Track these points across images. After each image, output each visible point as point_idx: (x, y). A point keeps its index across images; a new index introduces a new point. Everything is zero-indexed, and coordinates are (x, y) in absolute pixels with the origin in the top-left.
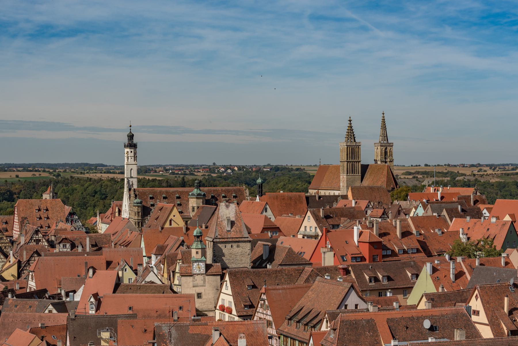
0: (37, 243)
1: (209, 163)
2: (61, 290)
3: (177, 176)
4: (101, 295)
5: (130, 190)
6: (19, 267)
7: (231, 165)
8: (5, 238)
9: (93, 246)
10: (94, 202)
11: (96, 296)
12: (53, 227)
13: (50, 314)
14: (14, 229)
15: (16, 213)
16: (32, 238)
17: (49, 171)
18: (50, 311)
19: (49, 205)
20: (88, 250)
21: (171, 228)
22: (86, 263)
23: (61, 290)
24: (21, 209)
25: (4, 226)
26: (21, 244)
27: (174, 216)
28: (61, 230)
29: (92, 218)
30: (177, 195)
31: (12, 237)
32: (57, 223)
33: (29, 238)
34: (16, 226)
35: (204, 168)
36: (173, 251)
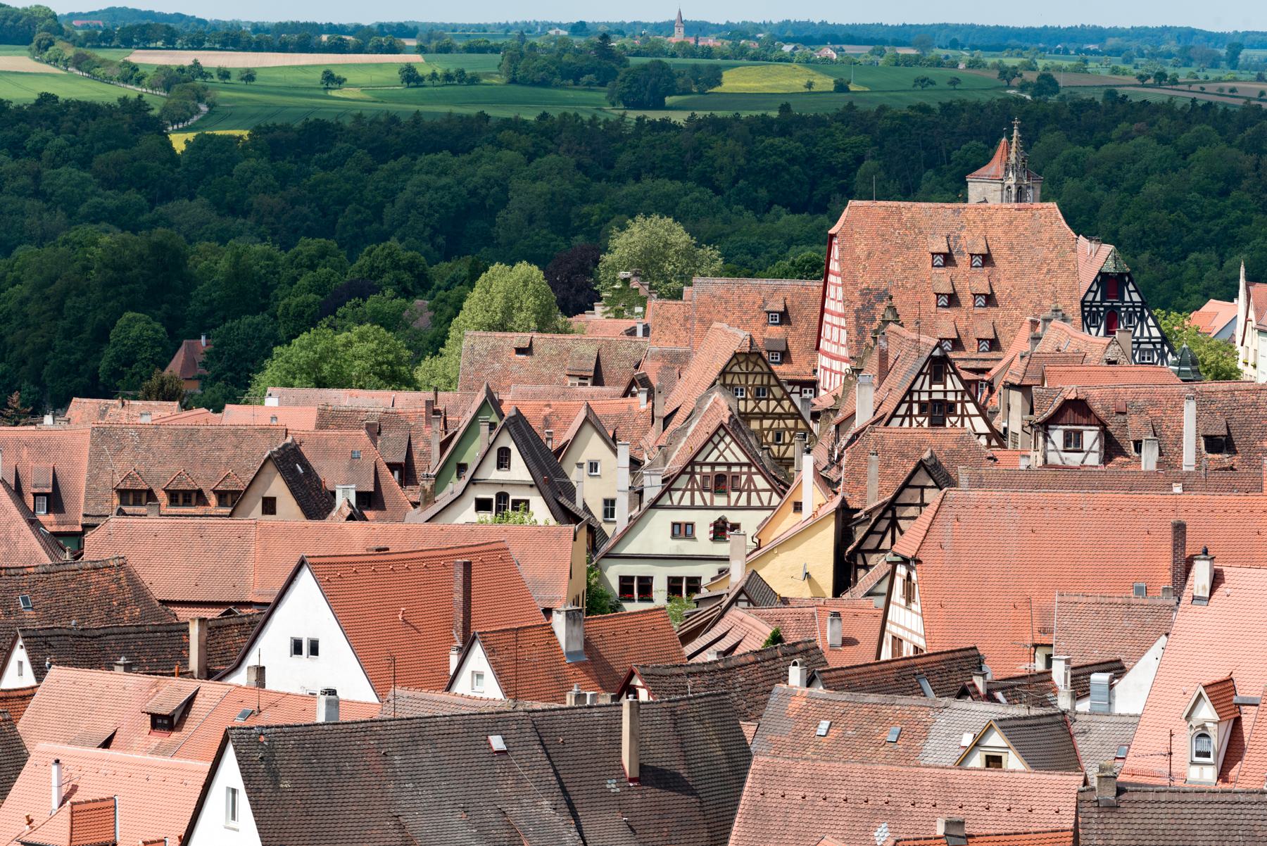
0: (937, 422)
2: (1049, 660)
4: (1245, 690)
6: (843, 537)
8: (777, 392)
9: (1214, 444)
10: (1224, 221)
11: (1222, 692)
12: (1017, 345)
13: (992, 774)
14: (824, 345)
15: (834, 266)
16: (910, 392)
18: (994, 761)
20: (1188, 459)
22: (1179, 529)
23: (1049, 660)
24: (861, 250)
25: (776, 332)
26: (858, 424)
28: (1059, 357)
29: (1213, 305)
31: (813, 385)
32: (1034, 324)
33: (899, 394)
34: (836, 336)
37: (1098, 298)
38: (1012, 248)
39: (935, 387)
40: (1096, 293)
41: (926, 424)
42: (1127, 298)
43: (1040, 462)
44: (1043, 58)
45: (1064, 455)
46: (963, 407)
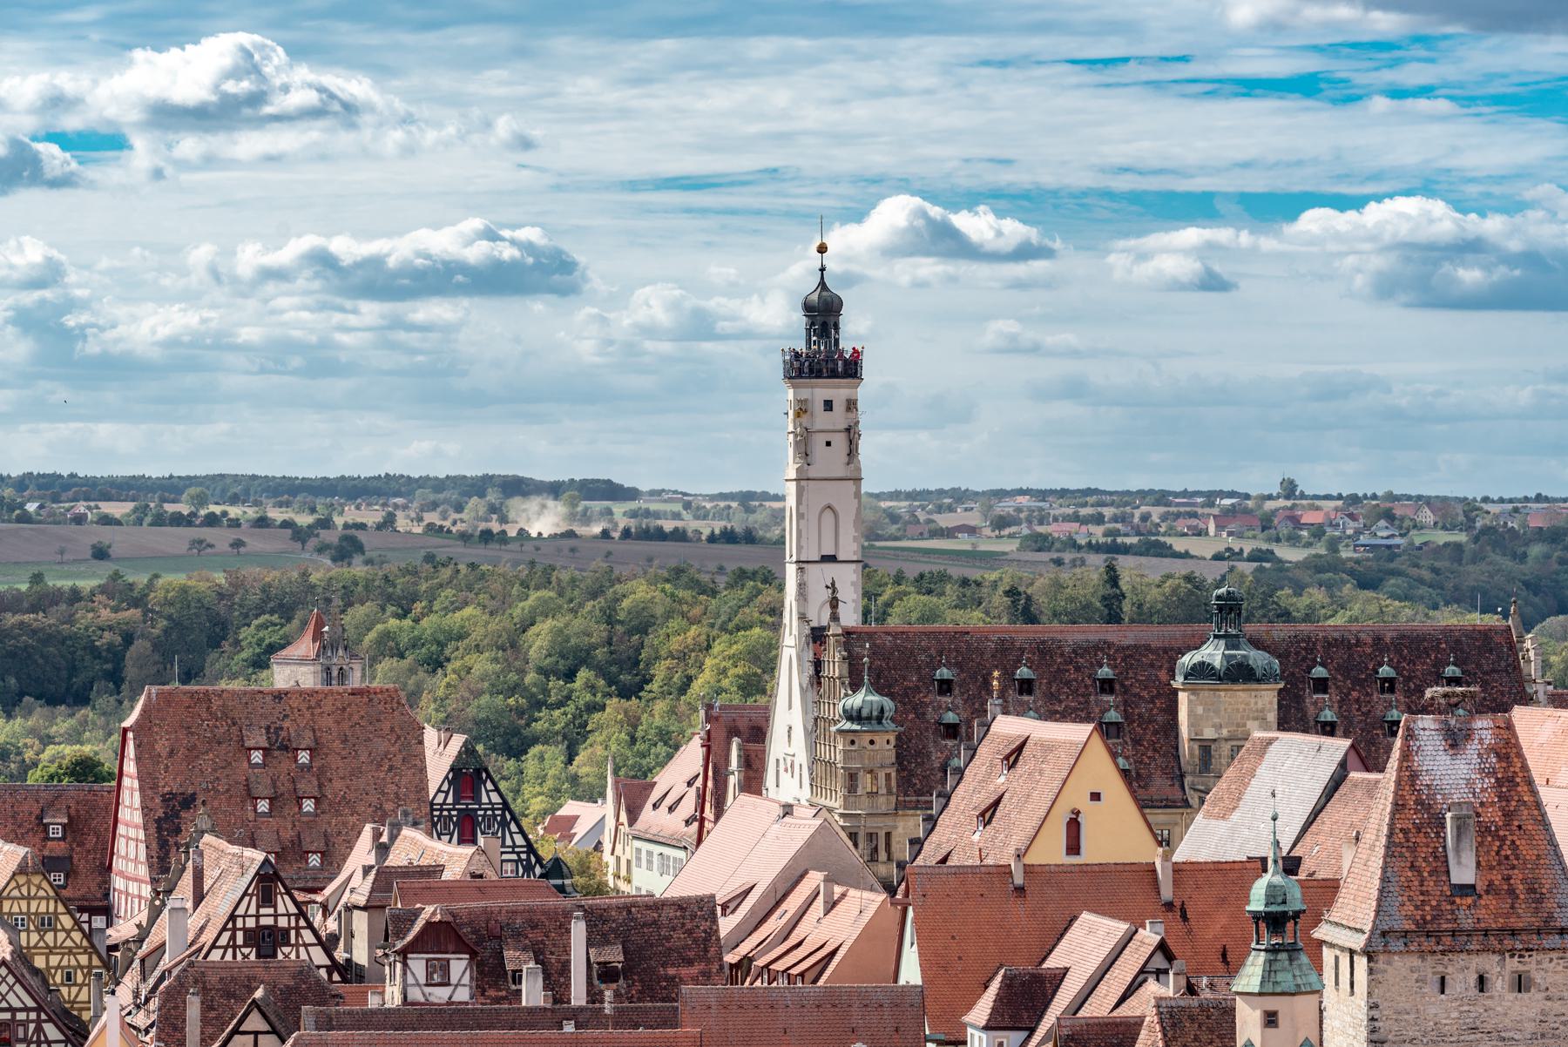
1: (1259, 480)
3: (1067, 557)
5: (818, 636)
7: (1391, 497)
17: (286, 524)
19: (327, 722)
20: (578, 995)
21: (1084, 869)
27: (1096, 797)
30: (1105, 672)
35: (1230, 513)
36: (1099, 1007)
37: (450, 800)
38: (345, 741)
39: (262, 911)
40: (447, 793)
41: (253, 957)
42: (485, 799)
43: (398, 1001)
44: (341, 513)
45: (428, 990)
46: (298, 935)
